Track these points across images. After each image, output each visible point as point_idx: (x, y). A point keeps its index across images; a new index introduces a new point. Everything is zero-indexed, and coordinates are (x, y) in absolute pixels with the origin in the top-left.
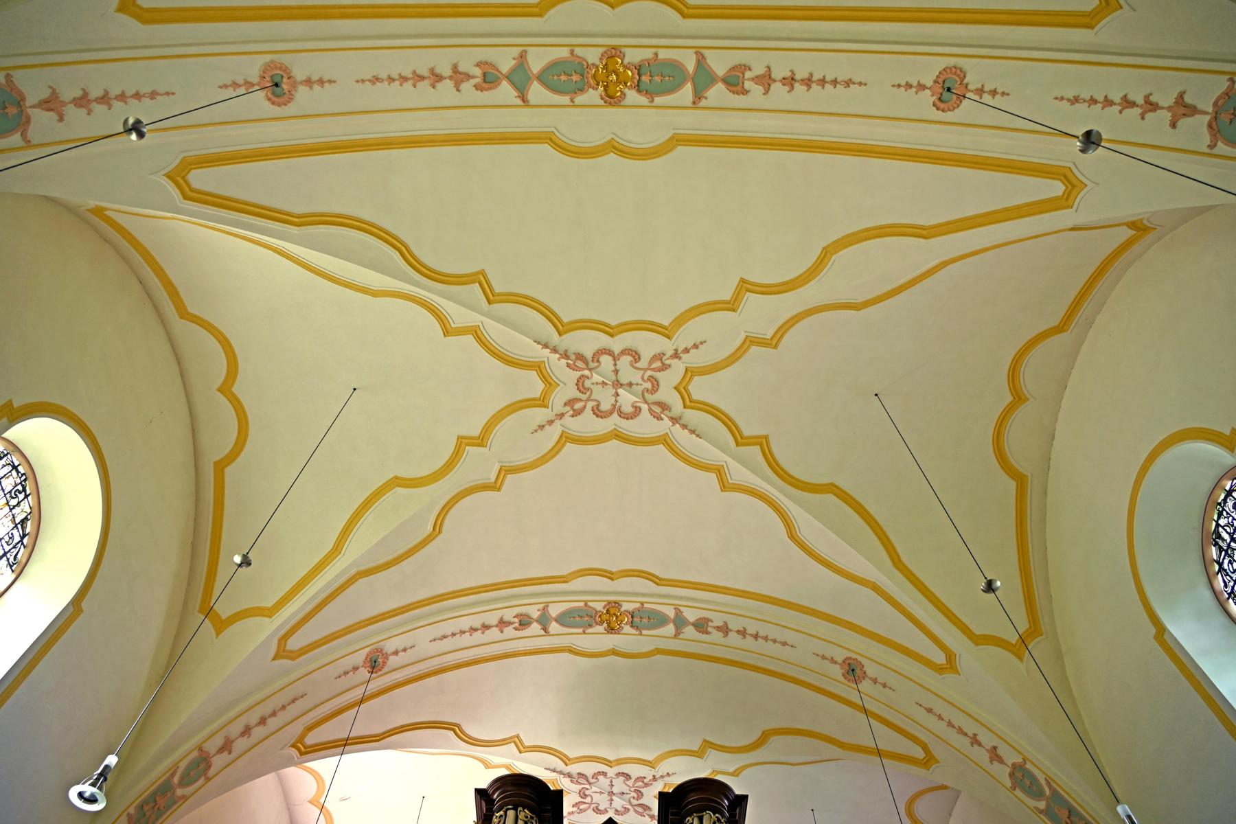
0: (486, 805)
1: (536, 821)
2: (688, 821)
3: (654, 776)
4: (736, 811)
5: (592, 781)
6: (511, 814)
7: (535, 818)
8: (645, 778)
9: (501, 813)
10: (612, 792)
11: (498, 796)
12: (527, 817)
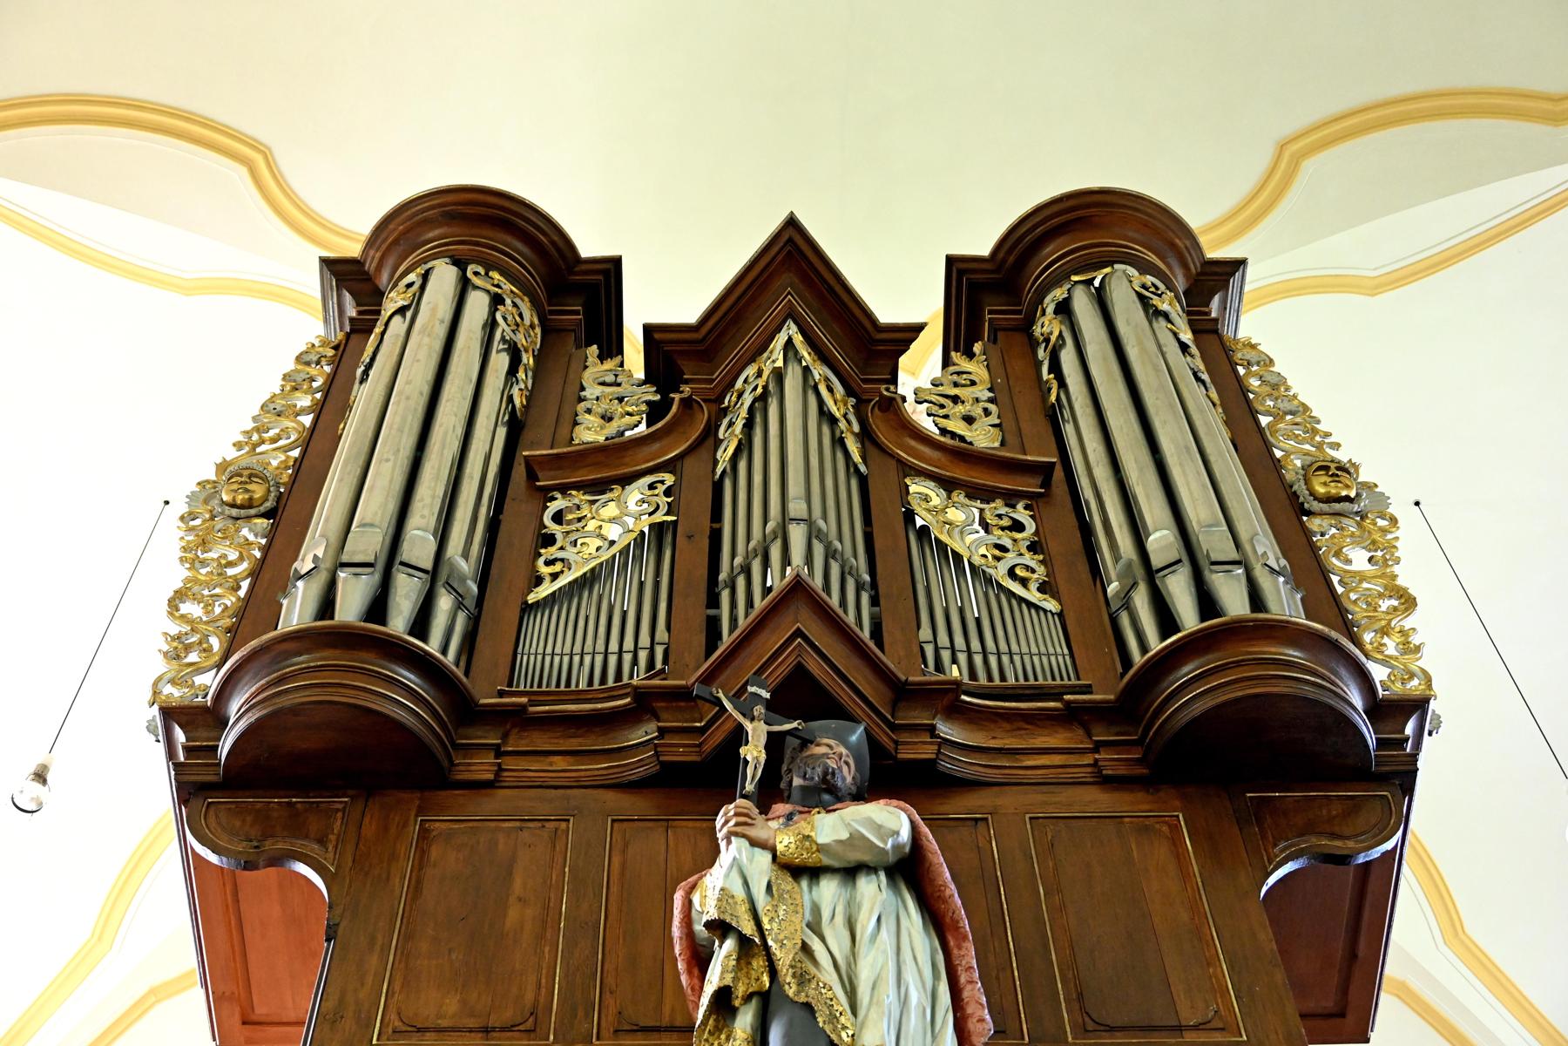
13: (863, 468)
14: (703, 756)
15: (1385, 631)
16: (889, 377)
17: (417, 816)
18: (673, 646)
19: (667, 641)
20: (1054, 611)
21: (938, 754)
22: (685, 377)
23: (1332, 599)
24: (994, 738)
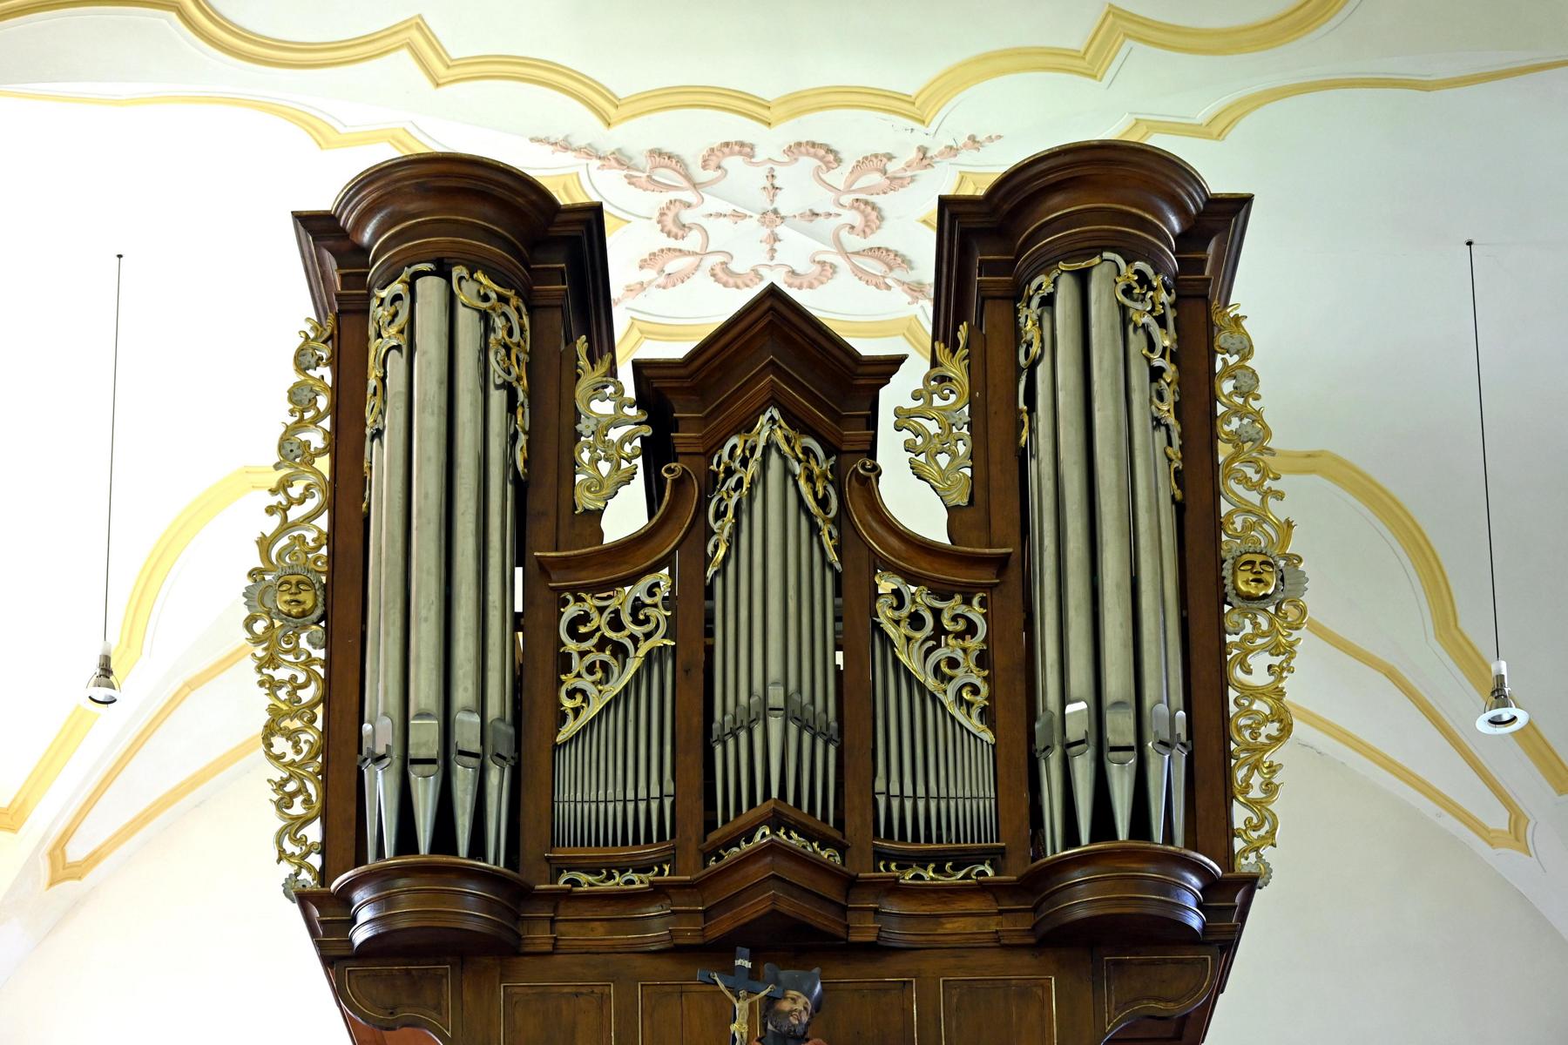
0: (340, 266)
1: (518, 309)
2: (1040, 287)
3: (923, 151)
4: (1205, 250)
5: (702, 176)
6: (430, 288)
7: (514, 301)
8: (890, 157)
9: (397, 287)
10: (775, 212)
11: (376, 236)
12: (486, 298)
13: (838, 566)
14: (706, 940)
15: (1255, 767)
16: (870, 412)
17: (501, 983)
18: (679, 799)
19: (672, 792)
20: (989, 742)
21: (879, 937)
22: (675, 415)
23: (1221, 729)
24: (923, 905)
